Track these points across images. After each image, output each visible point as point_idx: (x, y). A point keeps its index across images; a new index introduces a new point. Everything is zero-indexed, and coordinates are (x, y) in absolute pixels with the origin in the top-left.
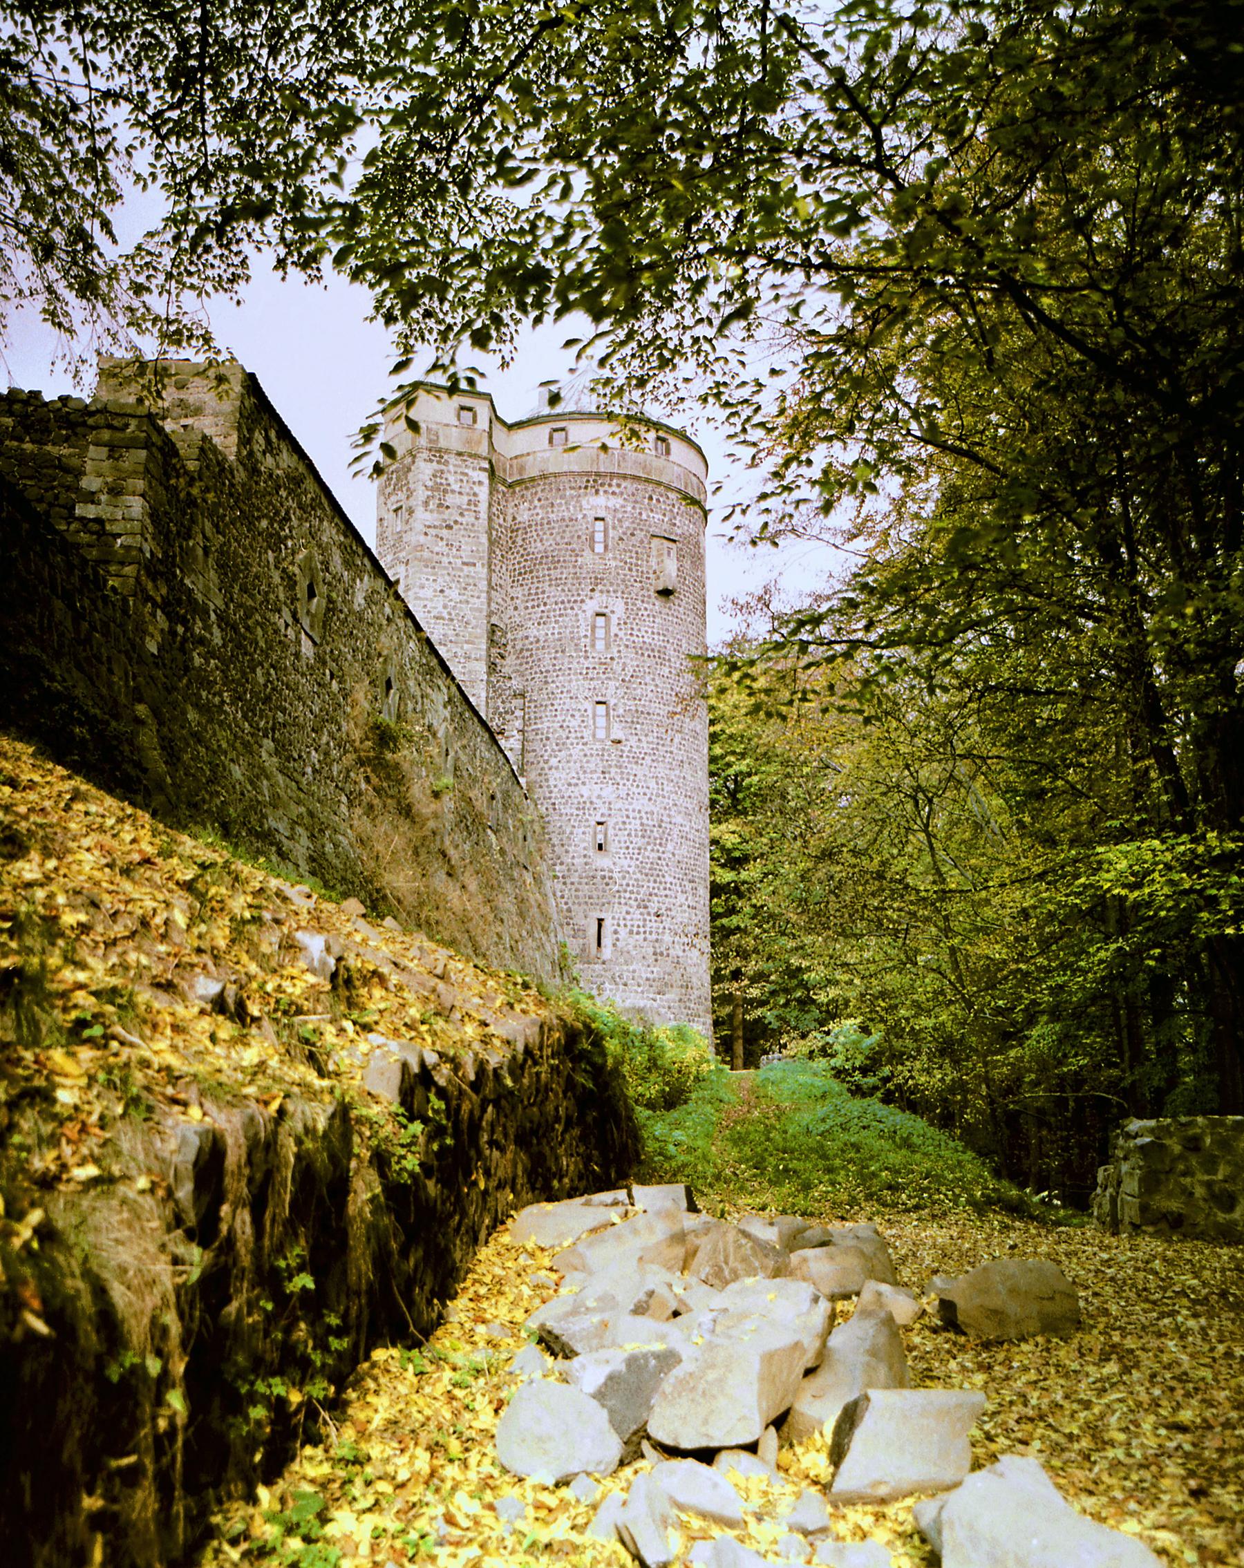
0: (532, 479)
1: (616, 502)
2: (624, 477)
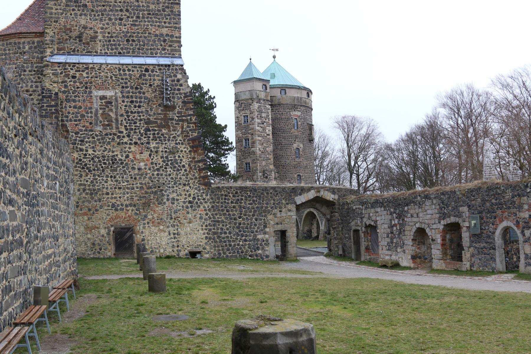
0: (275, 105)
1: (299, 114)
2: (301, 106)
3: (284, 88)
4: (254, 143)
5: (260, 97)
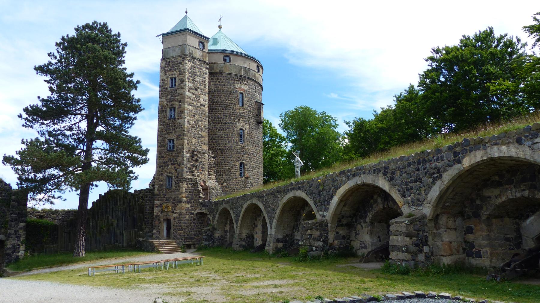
0: (216, 74)
1: (246, 88)
4: (182, 112)
5: (194, 55)
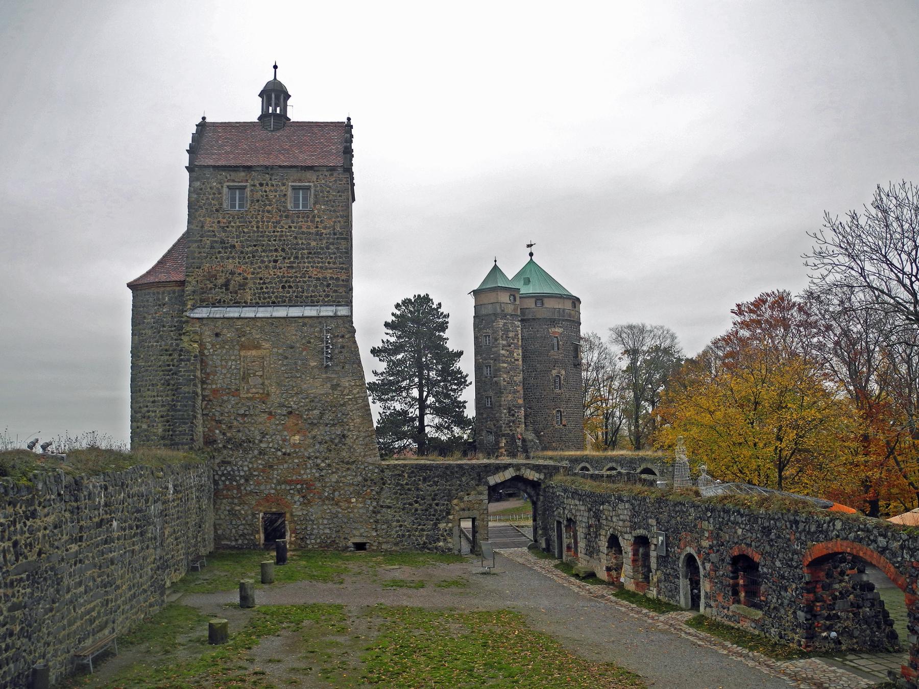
0: (529, 320)
2: (563, 320)
3: (540, 298)
5: (506, 311)
